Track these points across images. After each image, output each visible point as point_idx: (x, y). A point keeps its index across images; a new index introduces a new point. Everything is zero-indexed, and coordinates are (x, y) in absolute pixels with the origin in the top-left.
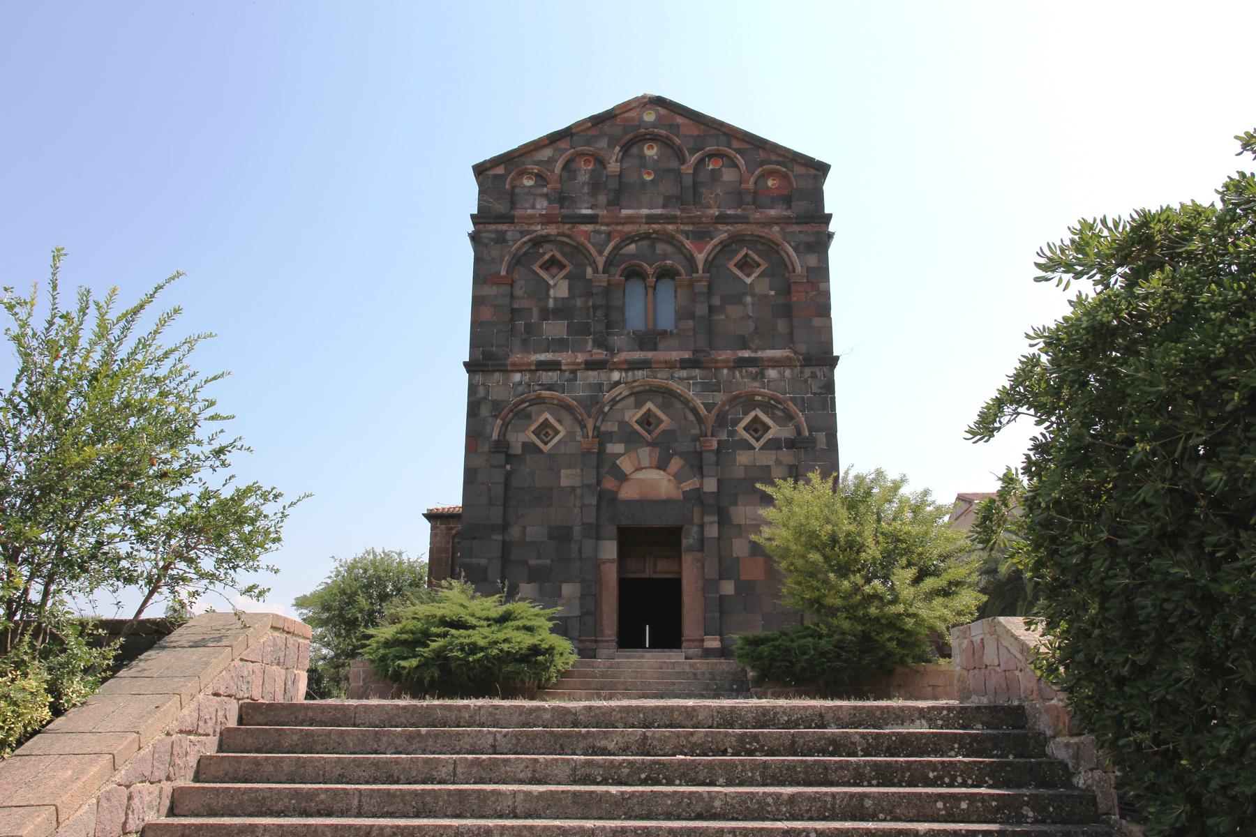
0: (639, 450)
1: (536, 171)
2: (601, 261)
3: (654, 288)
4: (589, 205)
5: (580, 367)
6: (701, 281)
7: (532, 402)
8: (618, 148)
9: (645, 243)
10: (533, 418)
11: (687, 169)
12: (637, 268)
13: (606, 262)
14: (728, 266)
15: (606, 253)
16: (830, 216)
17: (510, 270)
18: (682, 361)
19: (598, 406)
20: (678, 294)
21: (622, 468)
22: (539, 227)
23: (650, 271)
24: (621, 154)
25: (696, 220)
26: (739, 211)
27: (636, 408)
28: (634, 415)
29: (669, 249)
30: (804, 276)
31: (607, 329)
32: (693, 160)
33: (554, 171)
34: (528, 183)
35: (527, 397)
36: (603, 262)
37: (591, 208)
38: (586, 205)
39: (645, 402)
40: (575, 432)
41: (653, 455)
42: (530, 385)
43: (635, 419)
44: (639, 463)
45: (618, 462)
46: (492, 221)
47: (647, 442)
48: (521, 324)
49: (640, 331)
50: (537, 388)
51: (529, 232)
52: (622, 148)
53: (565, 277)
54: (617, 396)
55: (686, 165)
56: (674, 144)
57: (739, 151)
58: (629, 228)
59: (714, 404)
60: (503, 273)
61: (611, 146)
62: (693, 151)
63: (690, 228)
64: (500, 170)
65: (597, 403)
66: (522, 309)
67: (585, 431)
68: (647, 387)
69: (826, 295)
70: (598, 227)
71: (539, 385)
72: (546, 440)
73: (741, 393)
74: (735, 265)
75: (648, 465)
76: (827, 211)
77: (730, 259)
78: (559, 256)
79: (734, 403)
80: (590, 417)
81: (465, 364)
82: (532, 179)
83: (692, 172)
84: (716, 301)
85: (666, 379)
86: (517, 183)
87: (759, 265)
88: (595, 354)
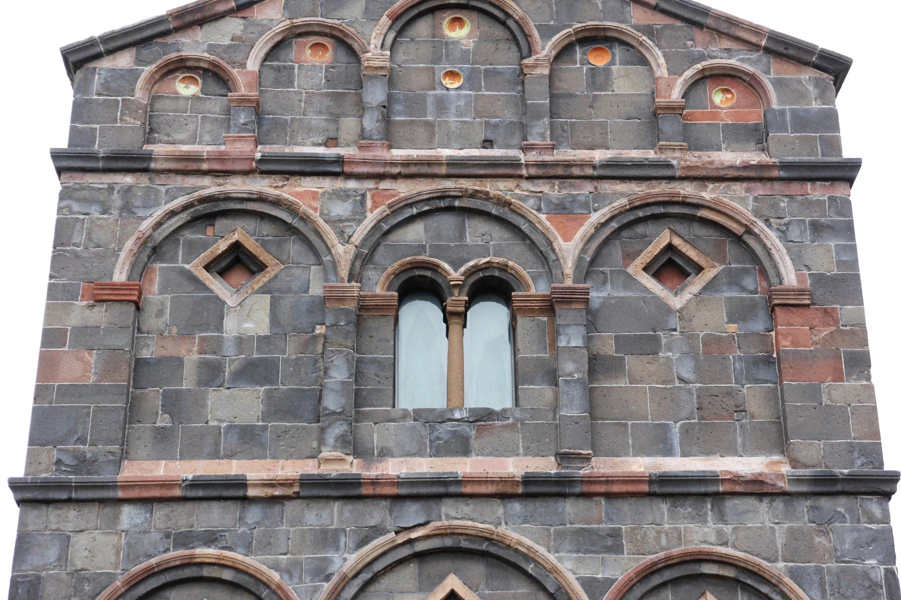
1: (205, 66)
2: (344, 253)
3: (463, 316)
4: (320, 140)
5: (289, 492)
6: (569, 301)
8: (385, 21)
9: (447, 222)
11: (535, 66)
12: (428, 274)
13: (357, 257)
14: (630, 270)
15: (357, 238)
16: (854, 166)
17: (140, 270)
18: (529, 480)
20: (519, 330)
22: (207, 181)
23: (455, 275)
24: (391, 36)
25: (560, 171)
26: (651, 155)
29: (497, 233)
30: (801, 292)
31: (357, 405)
32: (546, 49)
33: (243, 65)
34: (187, 89)
36: (350, 256)
37: (326, 144)
38: (315, 140)
39: (442, 578)
46: (101, 164)
48: (154, 396)
49: (432, 411)
51: (183, 191)
52: (395, 18)
53: (263, 290)
55: (534, 57)
56: (508, 15)
57: (649, 31)
58: (404, 189)
59: (610, 582)
60: (120, 276)
61: (371, 16)
62: (547, 32)
63: (543, 187)
64: (124, 60)
66: (160, 361)
68: (448, 542)
69: (859, 333)
70: (340, 184)
73: (668, 558)
74: (645, 269)
76: (848, 153)
77: (630, 257)
78: (251, 244)
79: (656, 580)
81: (15, 485)
82: (193, 80)
83: (546, 72)
84: (607, 345)
86: (163, 88)
87: (699, 269)
88: (327, 460)
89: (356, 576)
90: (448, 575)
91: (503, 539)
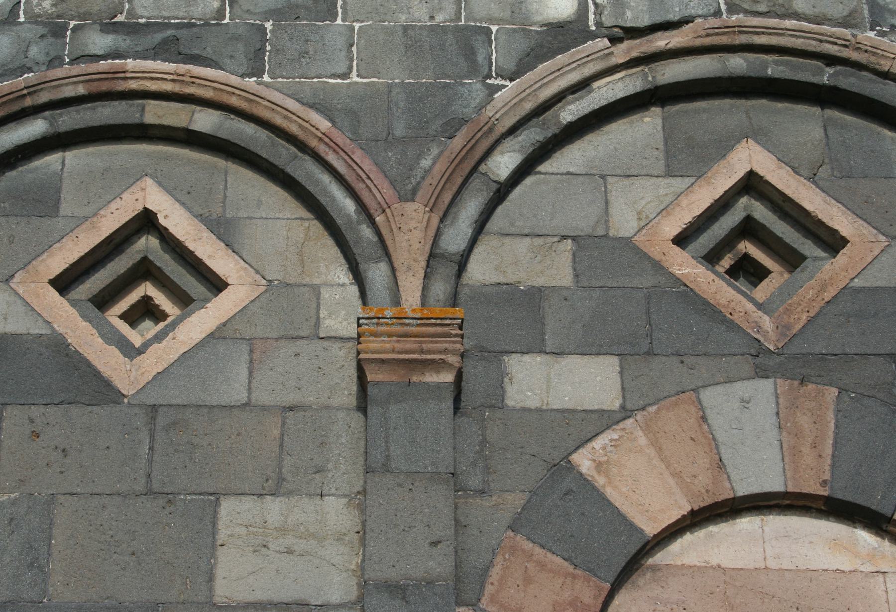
0: (709, 396)
7: (69, 120)
10: (65, 209)
19: (458, 142)
21: (611, 493)
27: (669, 173)
28: (664, 211)
35: (33, 89)
40: (316, 290)
41: (804, 421)
42: (57, 31)
43: (674, 226)
44: (721, 465)
45: (583, 461)
47: (758, 351)
50: (99, 42)
54: (559, 98)
65: (452, 128)
67: (377, 273)
68: (737, 64)
71: (111, 27)
72: (135, 337)
75: (774, 484)
80: (410, 196)
85: (845, 23)
89: (512, 131)
90: (738, 142)
91: (873, 59)
